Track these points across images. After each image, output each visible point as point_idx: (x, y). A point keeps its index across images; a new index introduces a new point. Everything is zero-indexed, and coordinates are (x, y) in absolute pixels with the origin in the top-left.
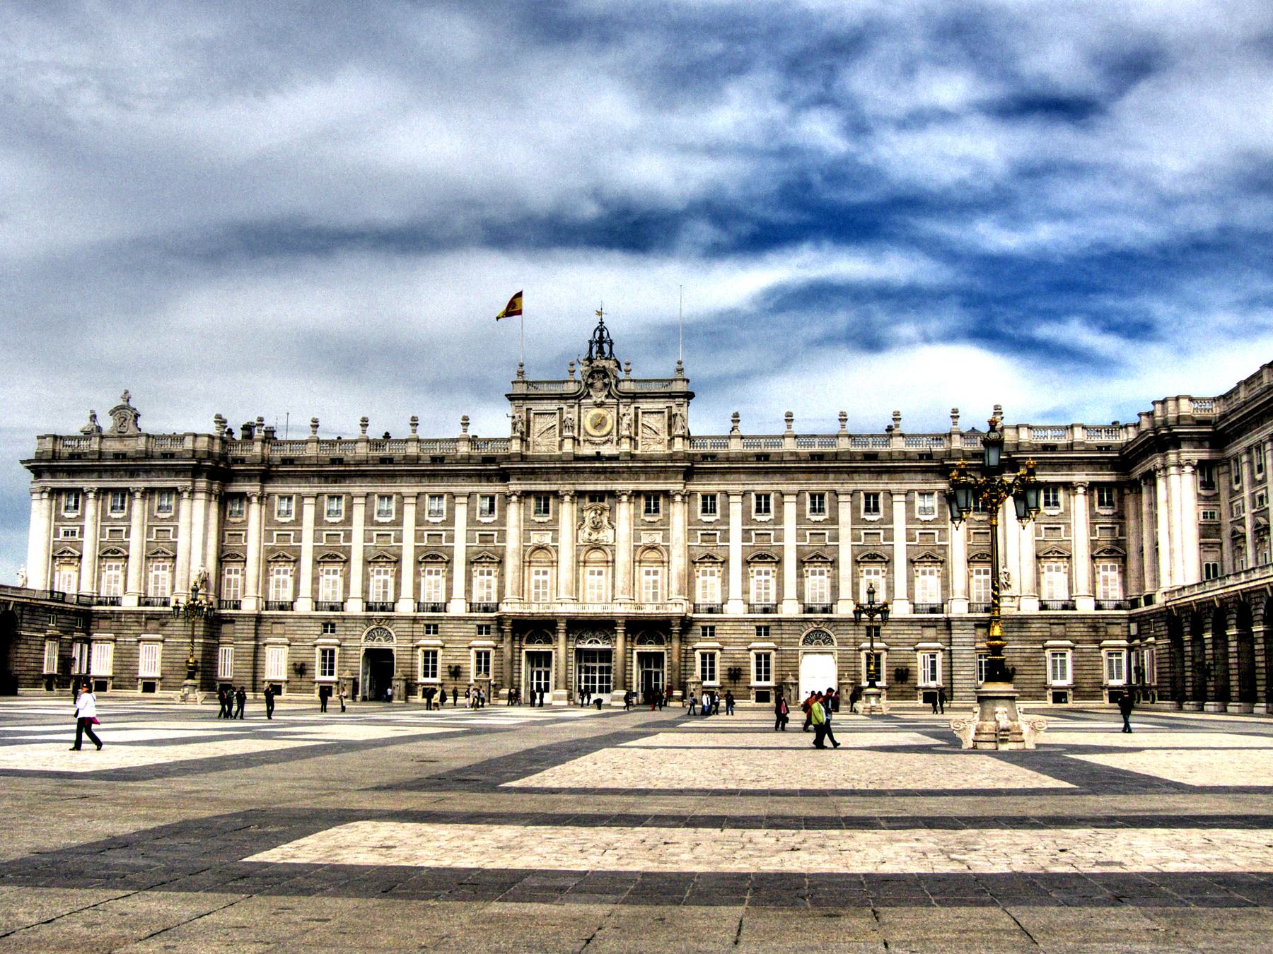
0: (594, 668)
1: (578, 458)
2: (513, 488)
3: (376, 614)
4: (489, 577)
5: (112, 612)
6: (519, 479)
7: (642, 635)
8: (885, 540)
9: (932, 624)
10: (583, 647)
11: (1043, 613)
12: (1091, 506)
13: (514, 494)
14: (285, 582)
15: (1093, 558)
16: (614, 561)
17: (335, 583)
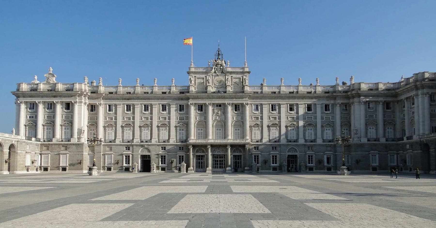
0: (218, 160)
1: (212, 93)
2: (191, 102)
3: (144, 143)
4: (183, 131)
5: (49, 144)
6: (192, 99)
7: (235, 150)
8: (314, 119)
9: (330, 146)
10: (215, 153)
11: (369, 142)
12: (384, 108)
13: (192, 104)
14: (111, 133)
15: (384, 125)
16: (225, 126)
17: (129, 133)
